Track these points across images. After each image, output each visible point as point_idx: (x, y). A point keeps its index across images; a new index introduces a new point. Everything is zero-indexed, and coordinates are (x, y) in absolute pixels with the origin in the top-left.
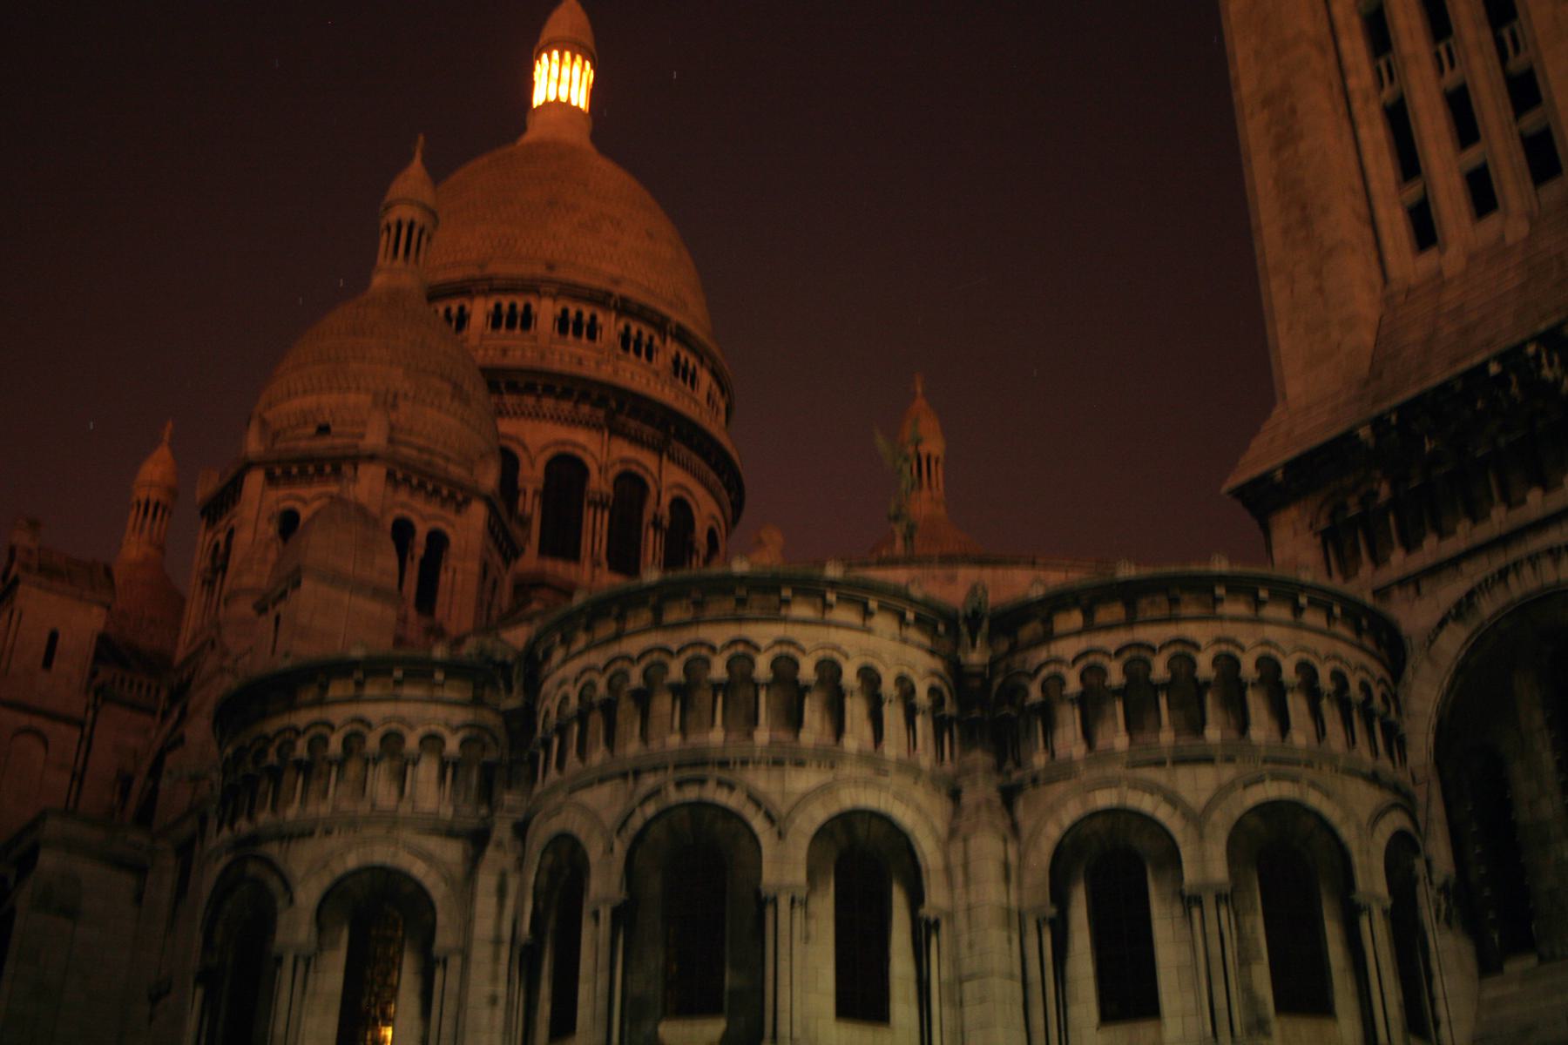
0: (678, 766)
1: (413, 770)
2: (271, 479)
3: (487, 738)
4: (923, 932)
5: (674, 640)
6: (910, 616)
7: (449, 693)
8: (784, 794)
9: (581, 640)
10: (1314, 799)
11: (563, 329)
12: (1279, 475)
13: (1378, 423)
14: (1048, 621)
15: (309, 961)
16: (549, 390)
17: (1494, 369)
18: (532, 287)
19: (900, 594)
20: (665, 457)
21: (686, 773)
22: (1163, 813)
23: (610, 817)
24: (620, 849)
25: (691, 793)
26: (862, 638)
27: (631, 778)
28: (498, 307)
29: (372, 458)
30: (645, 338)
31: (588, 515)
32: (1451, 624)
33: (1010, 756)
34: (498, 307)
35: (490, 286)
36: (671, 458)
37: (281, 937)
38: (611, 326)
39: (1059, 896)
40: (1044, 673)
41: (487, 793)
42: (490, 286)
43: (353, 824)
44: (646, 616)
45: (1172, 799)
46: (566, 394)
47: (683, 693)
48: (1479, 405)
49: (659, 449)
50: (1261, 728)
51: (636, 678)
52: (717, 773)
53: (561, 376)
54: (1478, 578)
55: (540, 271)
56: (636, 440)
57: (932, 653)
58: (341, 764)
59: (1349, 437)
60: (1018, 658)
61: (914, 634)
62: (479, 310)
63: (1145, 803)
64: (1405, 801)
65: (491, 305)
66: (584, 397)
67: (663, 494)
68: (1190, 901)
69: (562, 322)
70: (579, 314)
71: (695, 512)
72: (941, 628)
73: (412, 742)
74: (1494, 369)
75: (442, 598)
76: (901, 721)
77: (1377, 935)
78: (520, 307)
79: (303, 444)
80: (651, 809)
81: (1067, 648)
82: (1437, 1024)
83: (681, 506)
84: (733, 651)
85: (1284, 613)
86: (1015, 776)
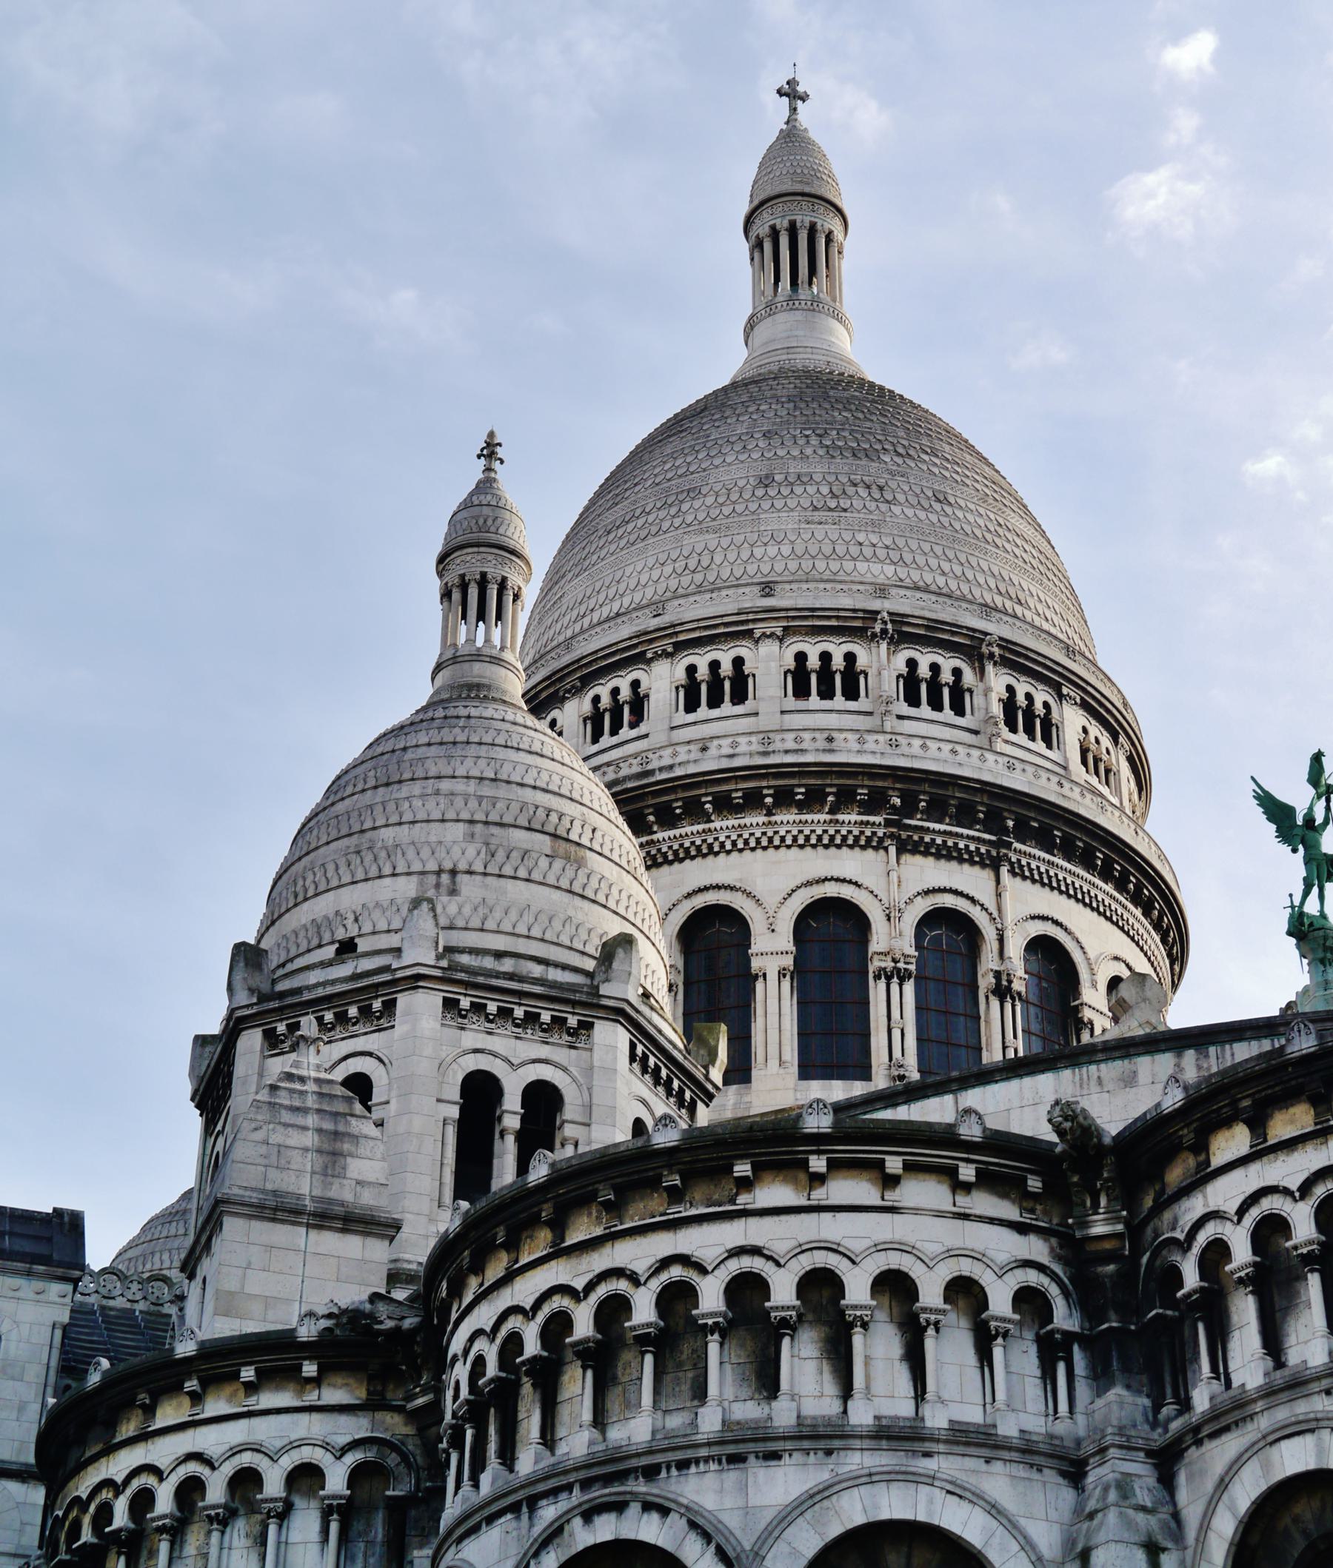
0: (586, 1484)
1: (280, 1526)
2: (272, 1040)
3: (392, 1460)
6: (967, 1173)
7: (333, 1395)
8: (746, 1510)
11: (801, 691)
14: (1201, 1147)
16: (784, 799)
18: (738, 629)
19: (944, 1137)
20: (1004, 870)
21: (598, 1493)
25: (606, 1529)
26: (882, 1227)
27: (525, 1509)
28: (691, 670)
30: (946, 677)
31: (877, 991)
33: (1169, 1391)
34: (691, 670)
36: (1017, 871)
40: (1202, 1238)
46: (813, 800)
49: (993, 864)
52: (640, 1487)
53: (802, 771)
55: (752, 599)
57: (1021, 1229)
58: (176, 1531)
60: (1167, 1216)
61: (983, 1203)
65: (680, 675)
66: (845, 799)
67: (1008, 934)
69: (799, 680)
70: (826, 657)
71: (1077, 956)
72: (1034, 1184)
73: (274, 1485)
76: (969, 1355)
78: (726, 669)
79: (314, 977)
84: (664, 1277)
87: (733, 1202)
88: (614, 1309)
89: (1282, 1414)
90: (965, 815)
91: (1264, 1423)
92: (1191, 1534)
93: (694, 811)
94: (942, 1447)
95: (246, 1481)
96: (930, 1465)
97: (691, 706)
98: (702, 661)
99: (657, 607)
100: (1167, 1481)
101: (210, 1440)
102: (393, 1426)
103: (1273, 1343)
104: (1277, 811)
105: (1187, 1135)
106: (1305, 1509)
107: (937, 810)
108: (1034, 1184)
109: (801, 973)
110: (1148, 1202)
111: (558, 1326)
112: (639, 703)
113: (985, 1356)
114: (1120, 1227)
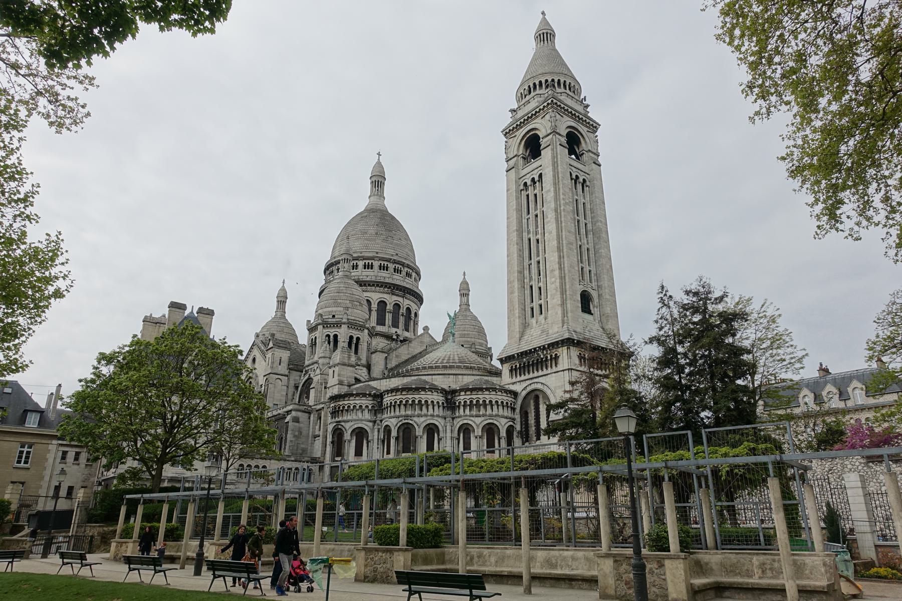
4: (439, 440)
5: (404, 397)
9: (390, 395)
10: (495, 422)
11: (380, 269)
13: (518, 354)
15: (350, 441)
16: (378, 286)
18: (372, 258)
22: (473, 425)
23: (395, 424)
24: (396, 428)
25: (406, 421)
29: (344, 323)
31: (387, 314)
35: (364, 258)
37: (345, 438)
38: (391, 266)
39: (459, 435)
41: (375, 415)
42: (364, 258)
43: (355, 420)
44: (399, 393)
45: (475, 423)
46: (382, 286)
47: (405, 405)
50: (489, 411)
51: (398, 403)
53: (380, 282)
56: (397, 295)
58: (353, 410)
59: (513, 355)
62: (361, 264)
64: (513, 420)
66: (386, 286)
68: (476, 437)
69: (380, 266)
73: (364, 407)
75: (359, 351)
80: (401, 423)
81: (462, 397)
83: (408, 309)
85: (494, 393)
88: (407, 401)
90: (400, 290)
93: (365, 285)
95: (361, 406)
97: (365, 268)
98: (367, 262)
99: (361, 253)
101: (356, 402)
102: (375, 402)
103: (464, 411)
104: (449, 316)
107: (397, 289)
109: (378, 311)
111: (401, 402)
112: (357, 266)
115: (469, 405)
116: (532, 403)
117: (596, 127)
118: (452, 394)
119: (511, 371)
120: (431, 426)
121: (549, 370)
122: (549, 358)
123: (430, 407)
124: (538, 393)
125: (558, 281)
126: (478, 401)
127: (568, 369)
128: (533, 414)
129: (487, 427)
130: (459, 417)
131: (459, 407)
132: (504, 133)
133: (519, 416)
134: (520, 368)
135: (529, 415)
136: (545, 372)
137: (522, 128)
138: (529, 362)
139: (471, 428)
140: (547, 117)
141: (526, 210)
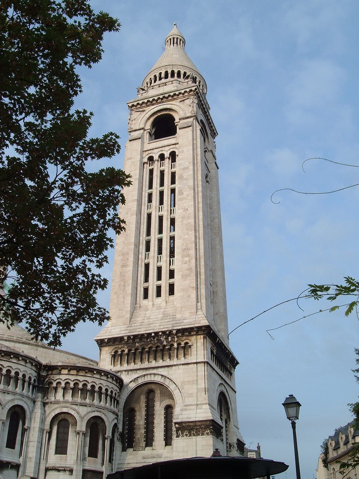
6: (34, 364)
10: (103, 416)
12: (106, 340)
13: (129, 337)
14: (60, 370)
17: (153, 335)
22: (76, 415)
32: (133, 382)
40: (58, 381)
45: (78, 413)
48: (148, 340)
50: (96, 402)
54: (140, 375)
57: (36, 372)
59: (122, 338)
63: (73, 412)
74: (153, 335)
77: (107, 443)
81: (63, 377)
82: (113, 460)
86: (47, 401)
87: (9, 360)
89: (64, 405)
91: (62, 405)
92: (47, 414)
94: (25, 397)
96: (23, 399)
100: (44, 406)
105: (60, 369)
106: (63, 415)
108: (38, 367)
110: (50, 373)
113: (29, 387)
114: (46, 375)
115: (73, 389)
116: (143, 399)
117: (215, 134)
118: (48, 371)
119: (114, 356)
120: (16, 409)
121: (175, 361)
122: (175, 345)
123: (20, 382)
124: (153, 387)
125: (194, 261)
126: (85, 385)
127: (204, 362)
128: (144, 413)
129: (92, 421)
130: (57, 402)
131: (56, 389)
132: (130, 105)
133: (122, 413)
134: (128, 354)
135: (137, 414)
136: (168, 362)
137: (153, 105)
138: (143, 349)
139: (70, 420)
140: (188, 102)
141: (147, 184)
